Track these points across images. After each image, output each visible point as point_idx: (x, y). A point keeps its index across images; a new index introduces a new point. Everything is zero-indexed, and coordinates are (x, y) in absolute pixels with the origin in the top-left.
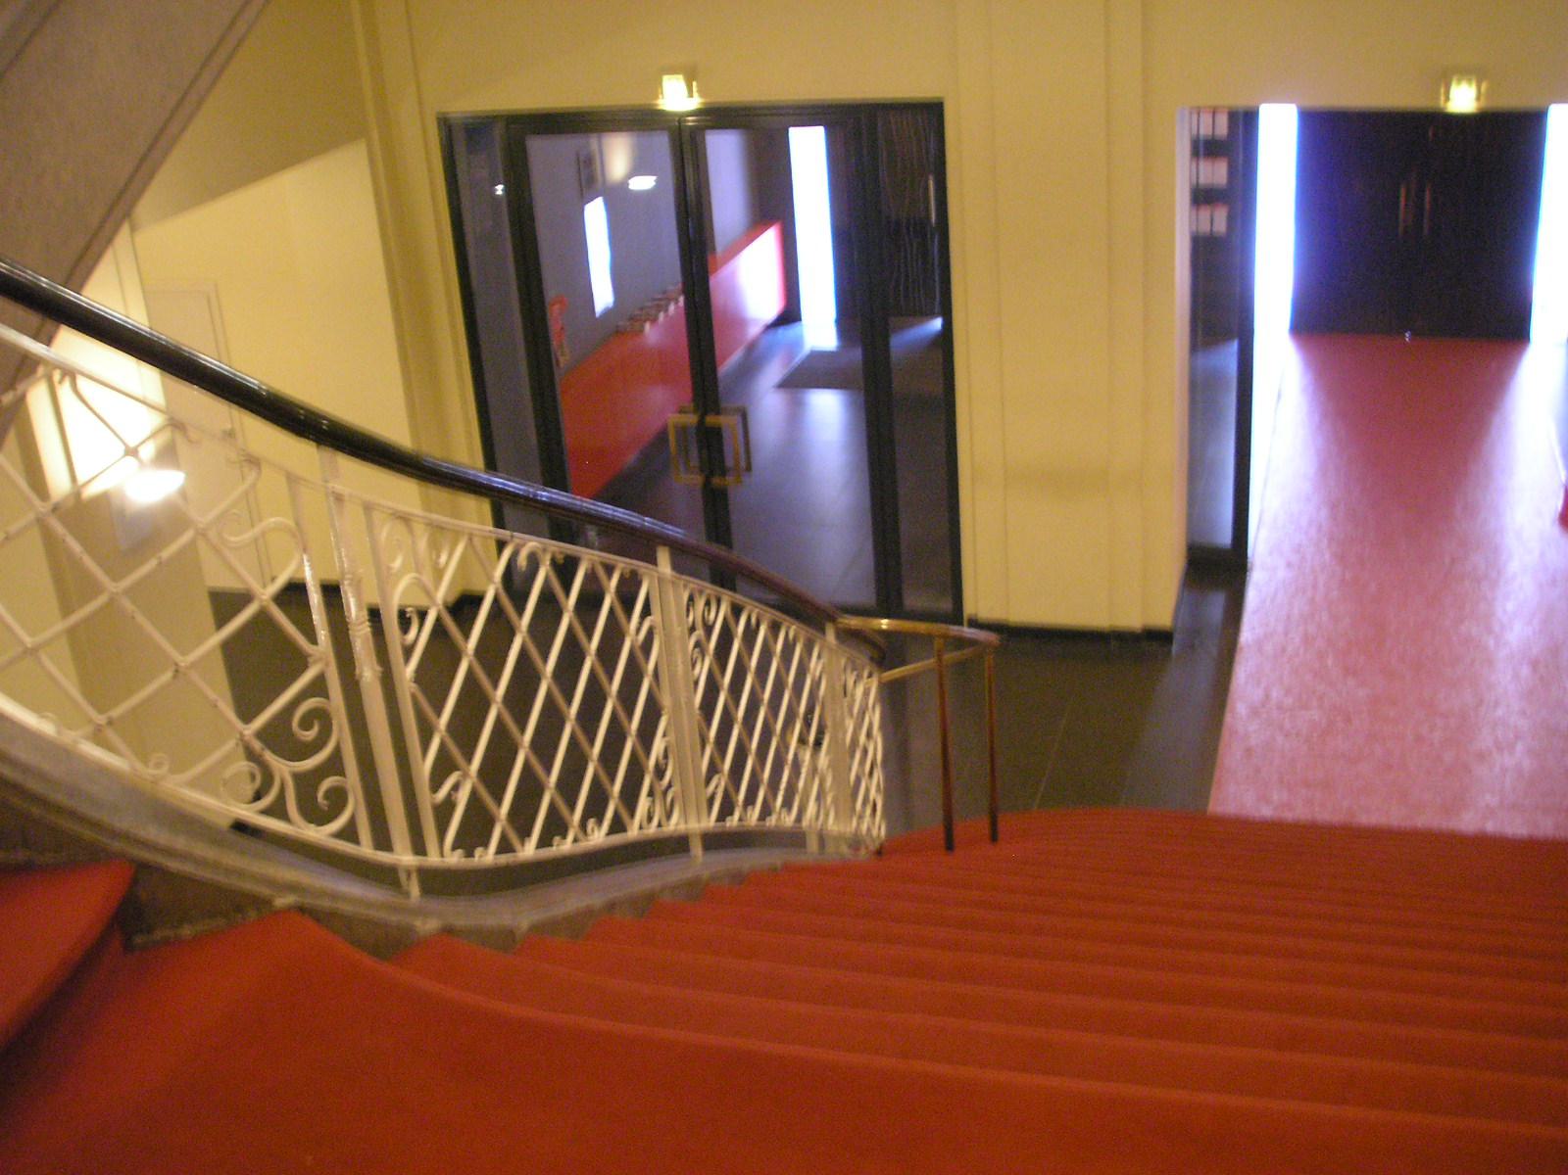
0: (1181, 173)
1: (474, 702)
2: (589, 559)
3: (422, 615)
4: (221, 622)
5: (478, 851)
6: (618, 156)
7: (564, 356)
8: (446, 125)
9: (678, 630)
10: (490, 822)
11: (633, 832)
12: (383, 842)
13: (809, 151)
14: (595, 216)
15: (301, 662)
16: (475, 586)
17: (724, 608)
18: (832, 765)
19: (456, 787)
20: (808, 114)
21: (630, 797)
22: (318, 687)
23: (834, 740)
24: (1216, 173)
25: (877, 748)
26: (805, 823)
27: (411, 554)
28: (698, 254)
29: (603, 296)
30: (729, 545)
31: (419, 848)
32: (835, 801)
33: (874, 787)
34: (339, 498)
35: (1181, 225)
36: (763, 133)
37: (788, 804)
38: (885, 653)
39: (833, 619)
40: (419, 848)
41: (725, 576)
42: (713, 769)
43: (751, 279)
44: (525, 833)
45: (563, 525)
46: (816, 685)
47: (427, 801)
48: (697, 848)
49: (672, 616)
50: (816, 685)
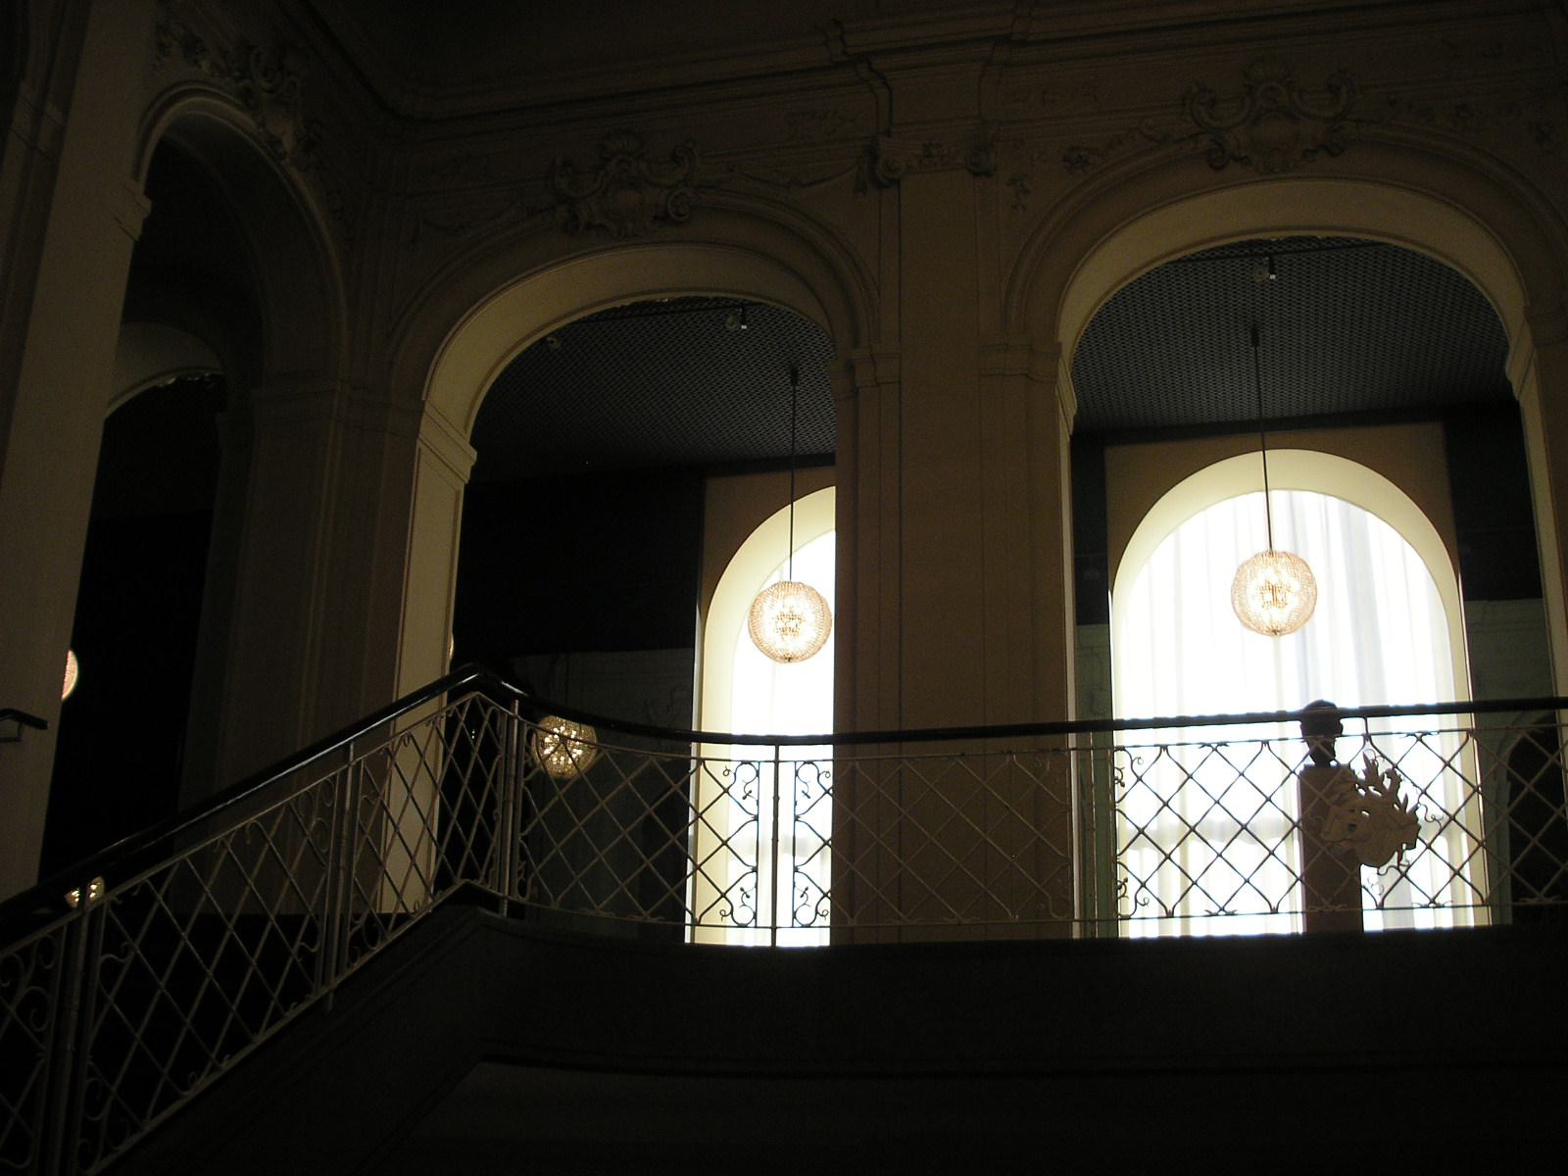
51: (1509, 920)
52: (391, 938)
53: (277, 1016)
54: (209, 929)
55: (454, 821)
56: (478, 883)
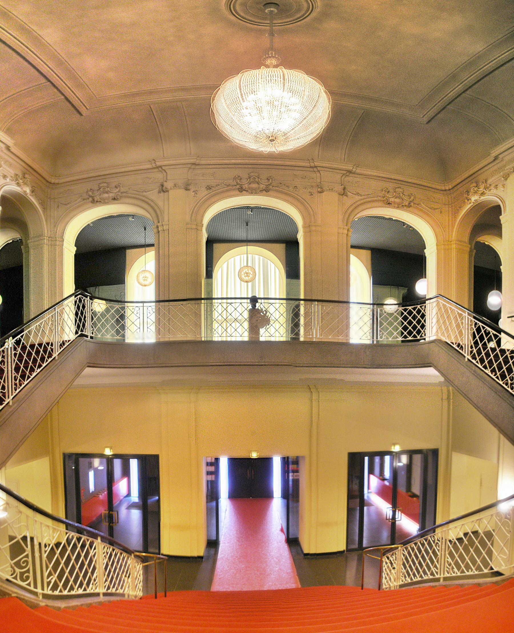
0: (204, 469)
1: (58, 563)
2: (84, 538)
3: (49, 545)
4: (10, 541)
5: (55, 591)
6: (96, 462)
7: (83, 499)
8: (64, 455)
9: (101, 553)
10: (58, 586)
11: (88, 591)
12: (36, 587)
13: (134, 464)
14: (91, 474)
15: (24, 551)
16: (61, 541)
17: (111, 549)
18: (132, 581)
19: (52, 579)
20: (134, 456)
21: (88, 584)
22: (27, 556)
23: (132, 577)
24: (212, 469)
25: (141, 578)
26: (125, 592)
27: (50, 534)
28: (111, 480)
29: (92, 488)
30: (113, 537)
31: (43, 589)
32: (132, 588)
33: (140, 586)
34: (36, 521)
35: (204, 479)
36: (125, 459)
37: (122, 588)
38: (144, 560)
39: (133, 553)
40: (43, 589)
41: (111, 543)
42: (106, 581)
43: (121, 487)
44: (65, 589)
45: (80, 531)
46: (129, 565)
47: (46, 581)
48: (101, 596)
49: (100, 550)
50: (129, 565)
51: (290, 340)
52: (67, 344)
53: (47, 361)
54: (32, 346)
55: (78, 321)
56: (83, 333)
